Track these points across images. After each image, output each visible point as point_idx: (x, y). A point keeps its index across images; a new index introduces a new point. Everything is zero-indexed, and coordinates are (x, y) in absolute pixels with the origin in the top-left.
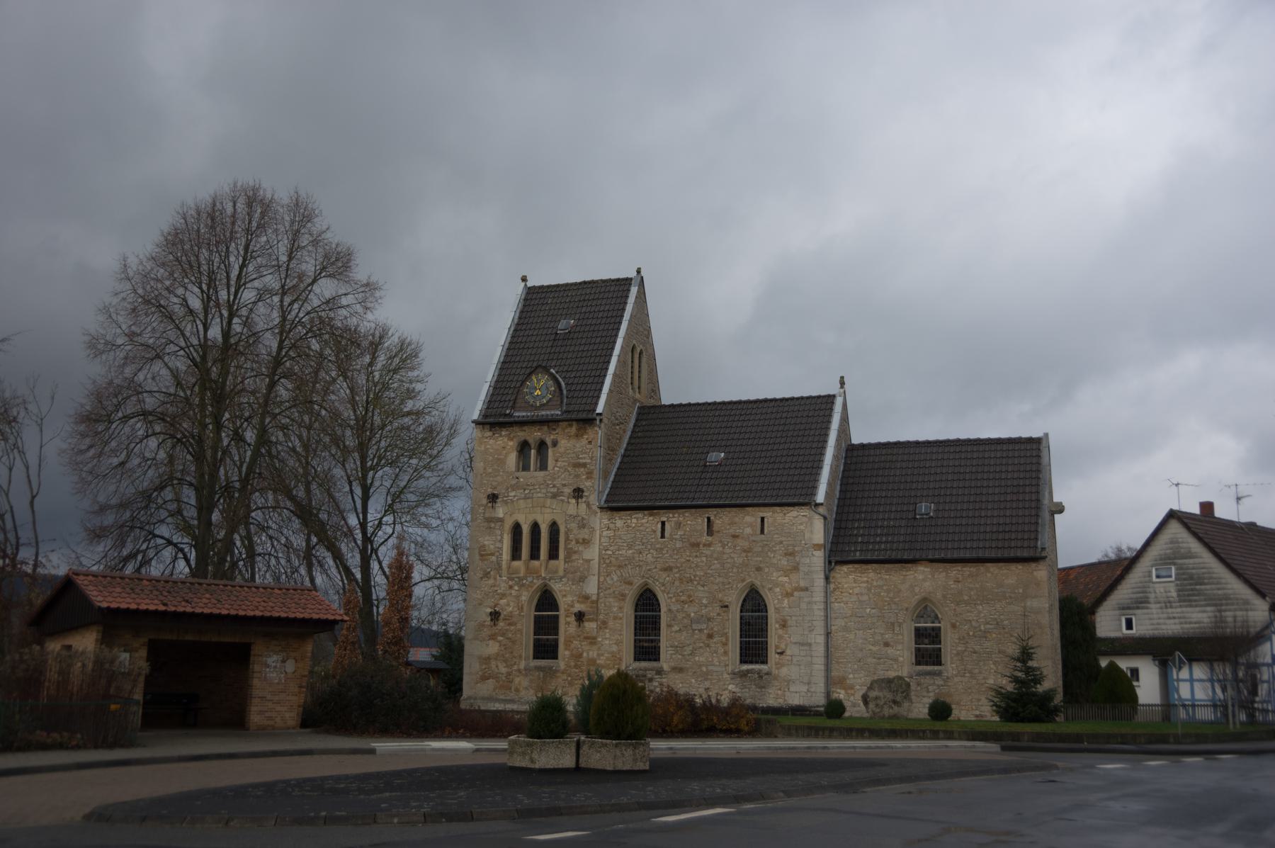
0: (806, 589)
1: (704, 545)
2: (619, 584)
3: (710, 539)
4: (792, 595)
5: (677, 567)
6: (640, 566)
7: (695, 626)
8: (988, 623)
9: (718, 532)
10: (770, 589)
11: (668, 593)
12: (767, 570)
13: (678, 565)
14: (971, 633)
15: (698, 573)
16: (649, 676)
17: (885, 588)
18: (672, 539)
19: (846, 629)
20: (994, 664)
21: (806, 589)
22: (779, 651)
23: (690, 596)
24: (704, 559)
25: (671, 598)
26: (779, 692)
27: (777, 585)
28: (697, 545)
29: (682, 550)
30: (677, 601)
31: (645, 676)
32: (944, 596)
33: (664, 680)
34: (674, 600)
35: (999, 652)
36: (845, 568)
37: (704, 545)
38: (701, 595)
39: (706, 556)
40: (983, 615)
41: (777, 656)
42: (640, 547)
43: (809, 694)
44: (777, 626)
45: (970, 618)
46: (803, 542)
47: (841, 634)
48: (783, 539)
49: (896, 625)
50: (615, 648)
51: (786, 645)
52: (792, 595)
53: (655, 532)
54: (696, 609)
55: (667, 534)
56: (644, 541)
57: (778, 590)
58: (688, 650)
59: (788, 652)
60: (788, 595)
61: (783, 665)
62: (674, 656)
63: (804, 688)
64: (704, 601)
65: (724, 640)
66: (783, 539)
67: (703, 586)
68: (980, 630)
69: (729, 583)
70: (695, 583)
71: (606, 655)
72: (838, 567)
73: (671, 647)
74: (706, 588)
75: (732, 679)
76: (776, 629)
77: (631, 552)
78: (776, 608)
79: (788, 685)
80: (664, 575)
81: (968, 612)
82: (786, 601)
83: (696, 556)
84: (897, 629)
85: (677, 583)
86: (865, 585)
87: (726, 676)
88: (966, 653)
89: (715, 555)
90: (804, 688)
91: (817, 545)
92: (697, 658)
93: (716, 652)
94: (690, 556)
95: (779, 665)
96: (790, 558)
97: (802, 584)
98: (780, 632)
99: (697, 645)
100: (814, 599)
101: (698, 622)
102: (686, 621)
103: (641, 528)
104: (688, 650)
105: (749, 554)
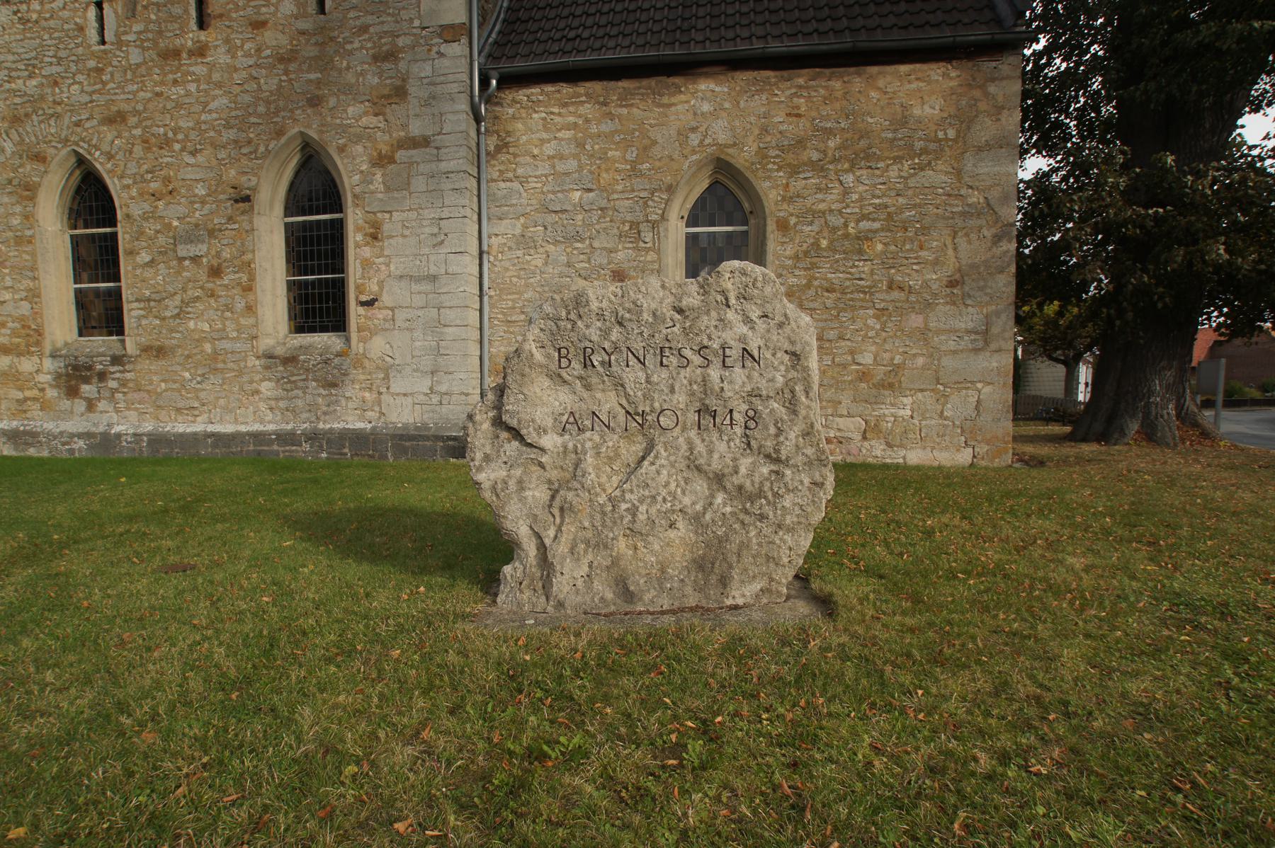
0: (423, 142)
1: (191, 53)
2: (17, 162)
3: (203, 36)
4: (392, 160)
5: (136, 113)
6: (57, 116)
7: (182, 251)
8: (865, 217)
9: (221, 16)
10: (341, 149)
11: (121, 177)
12: (332, 102)
13: (140, 107)
14: (824, 243)
15: (182, 124)
16: (99, 367)
17: (617, 138)
18: (120, 43)
19: (525, 242)
20: (877, 317)
21: (423, 142)
22: (364, 298)
23: (167, 180)
24: (192, 87)
25: (128, 187)
26: (367, 395)
27: (358, 139)
28: (176, 53)
29: (143, 70)
30: (141, 194)
31: (90, 368)
32: (762, 154)
33: (128, 376)
34: (134, 192)
35: (890, 287)
36: (522, 95)
37: (191, 53)
38: (190, 174)
39: (197, 81)
40: (855, 197)
41: (361, 310)
42: (55, 69)
43: (435, 399)
44: (359, 237)
45: (822, 206)
46: (417, 23)
47: (509, 255)
48: (369, 19)
49: (643, 227)
50: (25, 308)
51: (381, 284)
52: (392, 160)
53: (81, 29)
54: (182, 210)
55: (109, 36)
56: (62, 54)
57: (360, 149)
58: (173, 304)
59: (386, 299)
60: (382, 161)
61: (373, 333)
62: (144, 322)
63: (424, 385)
64: (201, 191)
65: (245, 278)
66: (369, 19)
67: (194, 153)
68: (846, 236)
69: (249, 142)
70: (177, 147)
71: (10, 325)
72: (508, 95)
73: (137, 300)
74: (200, 158)
75: (267, 368)
76: (357, 246)
77: (34, 82)
78: (355, 196)
79: (387, 377)
80: (109, 133)
81: (819, 190)
82: (379, 177)
83: (175, 82)
84: (648, 236)
85: (138, 151)
86: (566, 134)
87: (253, 362)
88: (812, 292)
89: (216, 76)
90: (424, 385)
91: (452, 26)
92: (191, 324)
93: (228, 308)
94: (162, 83)
95: (368, 332)
96: (387, 66)
97: (416, 129)
98: (367, 252)
99: (190, 293)
100: (444, 166)
101: (190, 239)
102: (162, 240)
103: (52, 23)
104: (173, 304)
105: (293, 66)
